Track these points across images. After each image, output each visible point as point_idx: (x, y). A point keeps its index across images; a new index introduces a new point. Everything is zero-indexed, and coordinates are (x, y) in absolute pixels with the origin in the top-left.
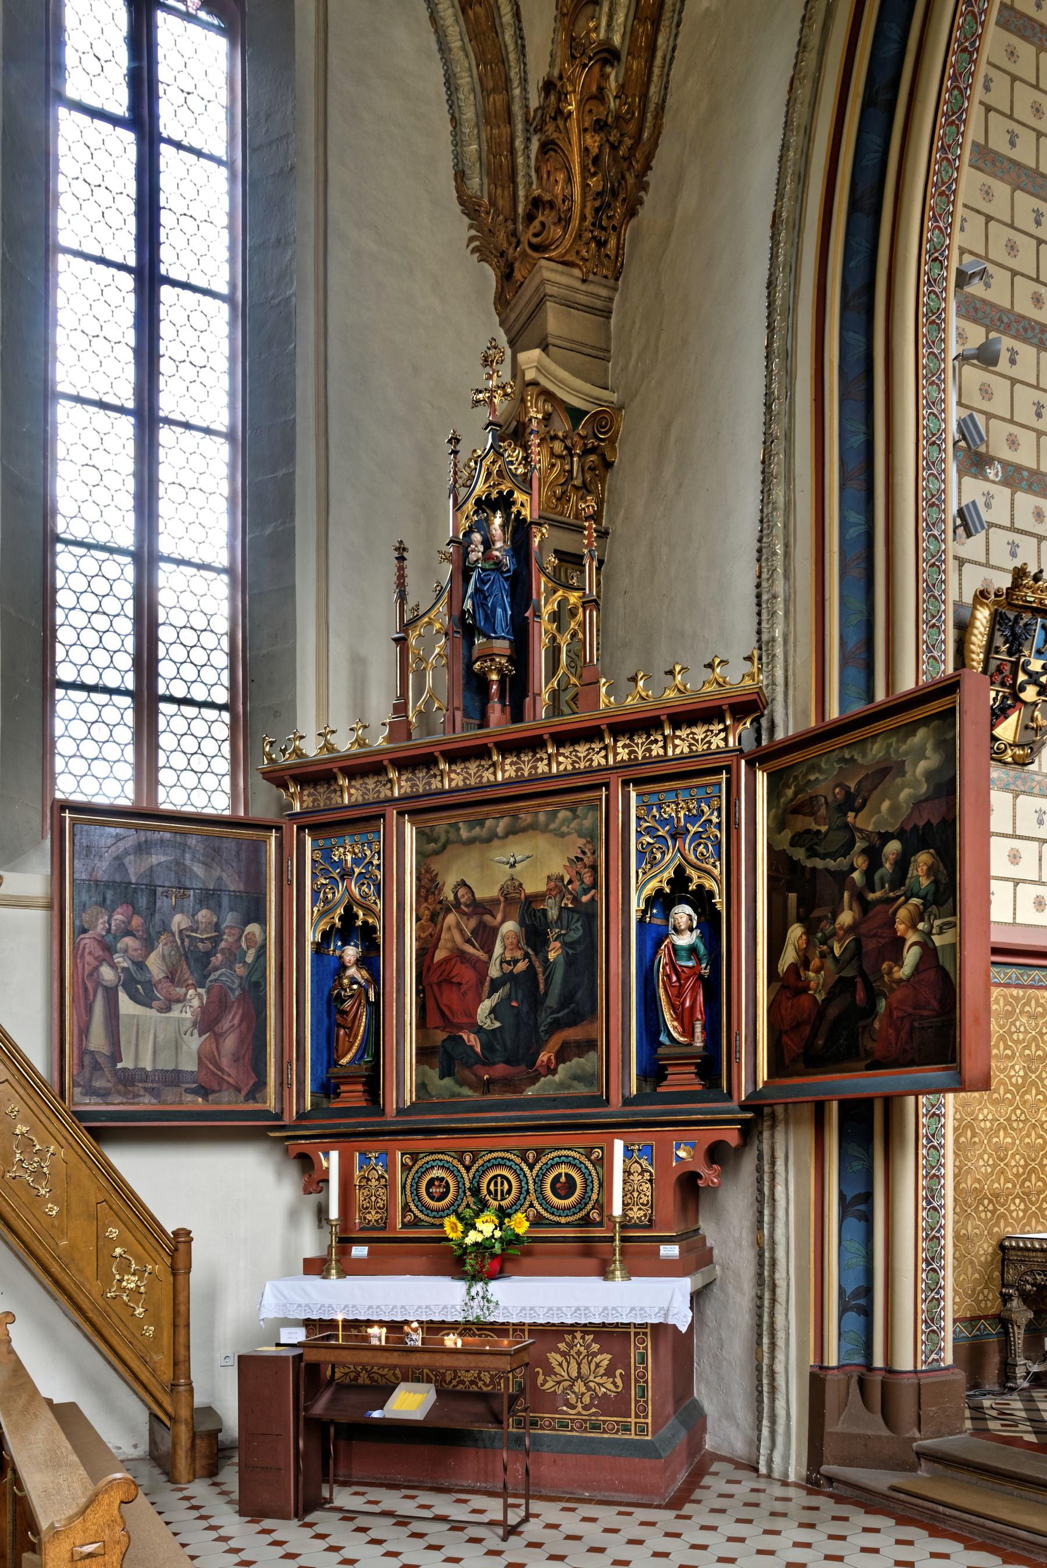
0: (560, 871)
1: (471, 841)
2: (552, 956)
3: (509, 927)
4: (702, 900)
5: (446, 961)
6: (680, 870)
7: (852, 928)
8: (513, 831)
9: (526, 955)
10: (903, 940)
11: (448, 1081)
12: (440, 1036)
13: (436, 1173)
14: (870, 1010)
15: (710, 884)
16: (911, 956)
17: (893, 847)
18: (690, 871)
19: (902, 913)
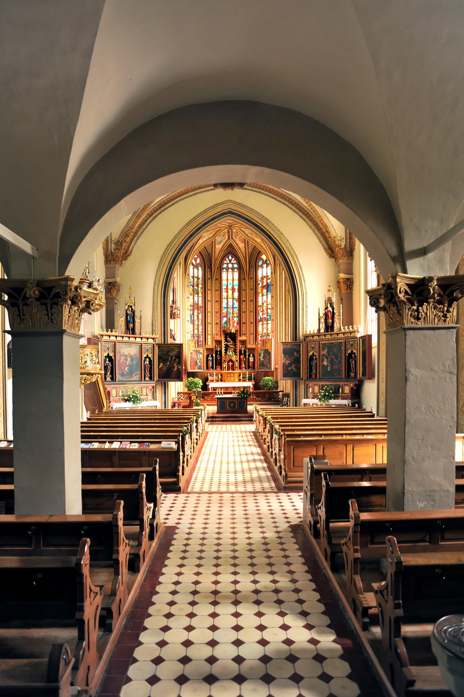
1: (125, 347)
3: (129, 359)
4: (150, 358)
8: (129, 347)
11: (122, 378)
12: (121, 372)
13: (122, 389)
14: (171, 373)
15: (151, 357)
16: (176, 368)
18: (149, 355)
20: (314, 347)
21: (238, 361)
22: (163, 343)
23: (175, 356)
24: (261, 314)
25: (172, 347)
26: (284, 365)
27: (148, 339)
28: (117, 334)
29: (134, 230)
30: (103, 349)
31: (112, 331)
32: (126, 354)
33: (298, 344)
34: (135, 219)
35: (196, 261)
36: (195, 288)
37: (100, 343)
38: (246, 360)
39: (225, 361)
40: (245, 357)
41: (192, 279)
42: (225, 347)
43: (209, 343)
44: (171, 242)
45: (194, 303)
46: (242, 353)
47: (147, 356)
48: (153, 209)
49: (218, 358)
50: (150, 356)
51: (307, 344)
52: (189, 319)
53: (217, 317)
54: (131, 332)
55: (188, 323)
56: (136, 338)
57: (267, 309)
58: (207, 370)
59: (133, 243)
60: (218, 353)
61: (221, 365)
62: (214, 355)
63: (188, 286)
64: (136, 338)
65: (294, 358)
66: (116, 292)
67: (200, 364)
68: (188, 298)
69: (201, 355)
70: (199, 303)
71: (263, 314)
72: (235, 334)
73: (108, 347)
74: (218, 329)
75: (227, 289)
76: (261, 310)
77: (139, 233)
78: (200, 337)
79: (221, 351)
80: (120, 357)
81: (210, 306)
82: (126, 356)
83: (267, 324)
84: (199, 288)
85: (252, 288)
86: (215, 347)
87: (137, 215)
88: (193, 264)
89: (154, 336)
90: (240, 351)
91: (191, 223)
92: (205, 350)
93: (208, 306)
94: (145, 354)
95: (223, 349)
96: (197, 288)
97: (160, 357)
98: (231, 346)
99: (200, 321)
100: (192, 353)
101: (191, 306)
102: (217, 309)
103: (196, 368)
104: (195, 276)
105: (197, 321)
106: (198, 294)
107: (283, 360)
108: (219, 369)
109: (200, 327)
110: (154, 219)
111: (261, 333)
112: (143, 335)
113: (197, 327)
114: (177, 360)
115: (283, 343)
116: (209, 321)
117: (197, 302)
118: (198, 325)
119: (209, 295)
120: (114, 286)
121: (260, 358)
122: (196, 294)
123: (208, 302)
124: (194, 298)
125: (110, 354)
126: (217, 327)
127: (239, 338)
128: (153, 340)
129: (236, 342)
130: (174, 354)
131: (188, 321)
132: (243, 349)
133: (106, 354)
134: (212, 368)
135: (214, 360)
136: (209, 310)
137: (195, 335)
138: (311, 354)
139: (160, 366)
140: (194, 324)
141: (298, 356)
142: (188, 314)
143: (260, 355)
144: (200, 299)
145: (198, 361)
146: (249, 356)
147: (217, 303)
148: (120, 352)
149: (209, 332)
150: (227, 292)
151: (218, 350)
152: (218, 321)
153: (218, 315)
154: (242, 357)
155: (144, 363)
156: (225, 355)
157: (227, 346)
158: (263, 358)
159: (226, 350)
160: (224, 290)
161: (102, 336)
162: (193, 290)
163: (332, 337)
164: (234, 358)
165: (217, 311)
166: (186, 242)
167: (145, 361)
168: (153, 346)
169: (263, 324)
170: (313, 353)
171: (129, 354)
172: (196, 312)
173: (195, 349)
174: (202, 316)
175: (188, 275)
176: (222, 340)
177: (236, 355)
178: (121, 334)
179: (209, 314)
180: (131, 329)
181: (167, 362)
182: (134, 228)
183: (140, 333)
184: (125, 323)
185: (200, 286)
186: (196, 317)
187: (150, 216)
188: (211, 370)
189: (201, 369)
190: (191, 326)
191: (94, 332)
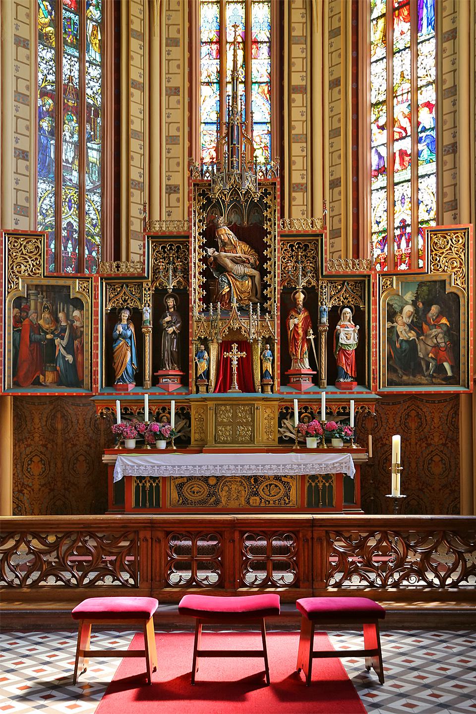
21: (277, 338)
24: (379, 138)
42: (203, 273)
45: (58, 81)
53: (173, 162)
55: (22, 163)
57: (414, 108)
58: (110, 390)
60: (171, 302)
61: (183, 360)
67: (69, 358)
69: (76, 313)
70: (89, 91)
71: (392, 140)
75: (220, 41)
76: (382, 122)
81: (142, 112)
83: (416, 178)
84: (90, 25)
85: (336, 25)
86: (156, 271)
90: (288, 293)
92: (101, 287)
93: (132, 105)
95: (196, 282)
98: (240, 269)
102: (173, 127)
103: (50, 377)
106: (81, 45)
108: (174, 386)
111: (383, 225)
116: (135, 175)
119: (136, 61)
121: (391, 330)
122: (72, 45)
123: (132, 90)
124: (58, 60)
126: (173, 203)
129: (266, 246)
131: (22, 155)
132: (302, 283)
136: (136, 126)
137: (64, 233)
140: (58, 181)
142: (22, 124)
143: (392, 315)
144: (95, 72)
145: (60, 344)
146: (335, 315)
147: (174, 99)
150: (221, 54)
154: (297, 321)
156: (206, 311)
159: (211, 295)
160: (205, 49)
165: (173, 132)
169: (391, 186)
172: (70, 127)
173: (45, 282)
174: (102, 151)
176: (188, 237)
177: (264, 311)
179: (135, 144)
185: (94, 13)
186: (68, 154)
188: (131, 387)
189: (79, 384)
190: (44, 187)
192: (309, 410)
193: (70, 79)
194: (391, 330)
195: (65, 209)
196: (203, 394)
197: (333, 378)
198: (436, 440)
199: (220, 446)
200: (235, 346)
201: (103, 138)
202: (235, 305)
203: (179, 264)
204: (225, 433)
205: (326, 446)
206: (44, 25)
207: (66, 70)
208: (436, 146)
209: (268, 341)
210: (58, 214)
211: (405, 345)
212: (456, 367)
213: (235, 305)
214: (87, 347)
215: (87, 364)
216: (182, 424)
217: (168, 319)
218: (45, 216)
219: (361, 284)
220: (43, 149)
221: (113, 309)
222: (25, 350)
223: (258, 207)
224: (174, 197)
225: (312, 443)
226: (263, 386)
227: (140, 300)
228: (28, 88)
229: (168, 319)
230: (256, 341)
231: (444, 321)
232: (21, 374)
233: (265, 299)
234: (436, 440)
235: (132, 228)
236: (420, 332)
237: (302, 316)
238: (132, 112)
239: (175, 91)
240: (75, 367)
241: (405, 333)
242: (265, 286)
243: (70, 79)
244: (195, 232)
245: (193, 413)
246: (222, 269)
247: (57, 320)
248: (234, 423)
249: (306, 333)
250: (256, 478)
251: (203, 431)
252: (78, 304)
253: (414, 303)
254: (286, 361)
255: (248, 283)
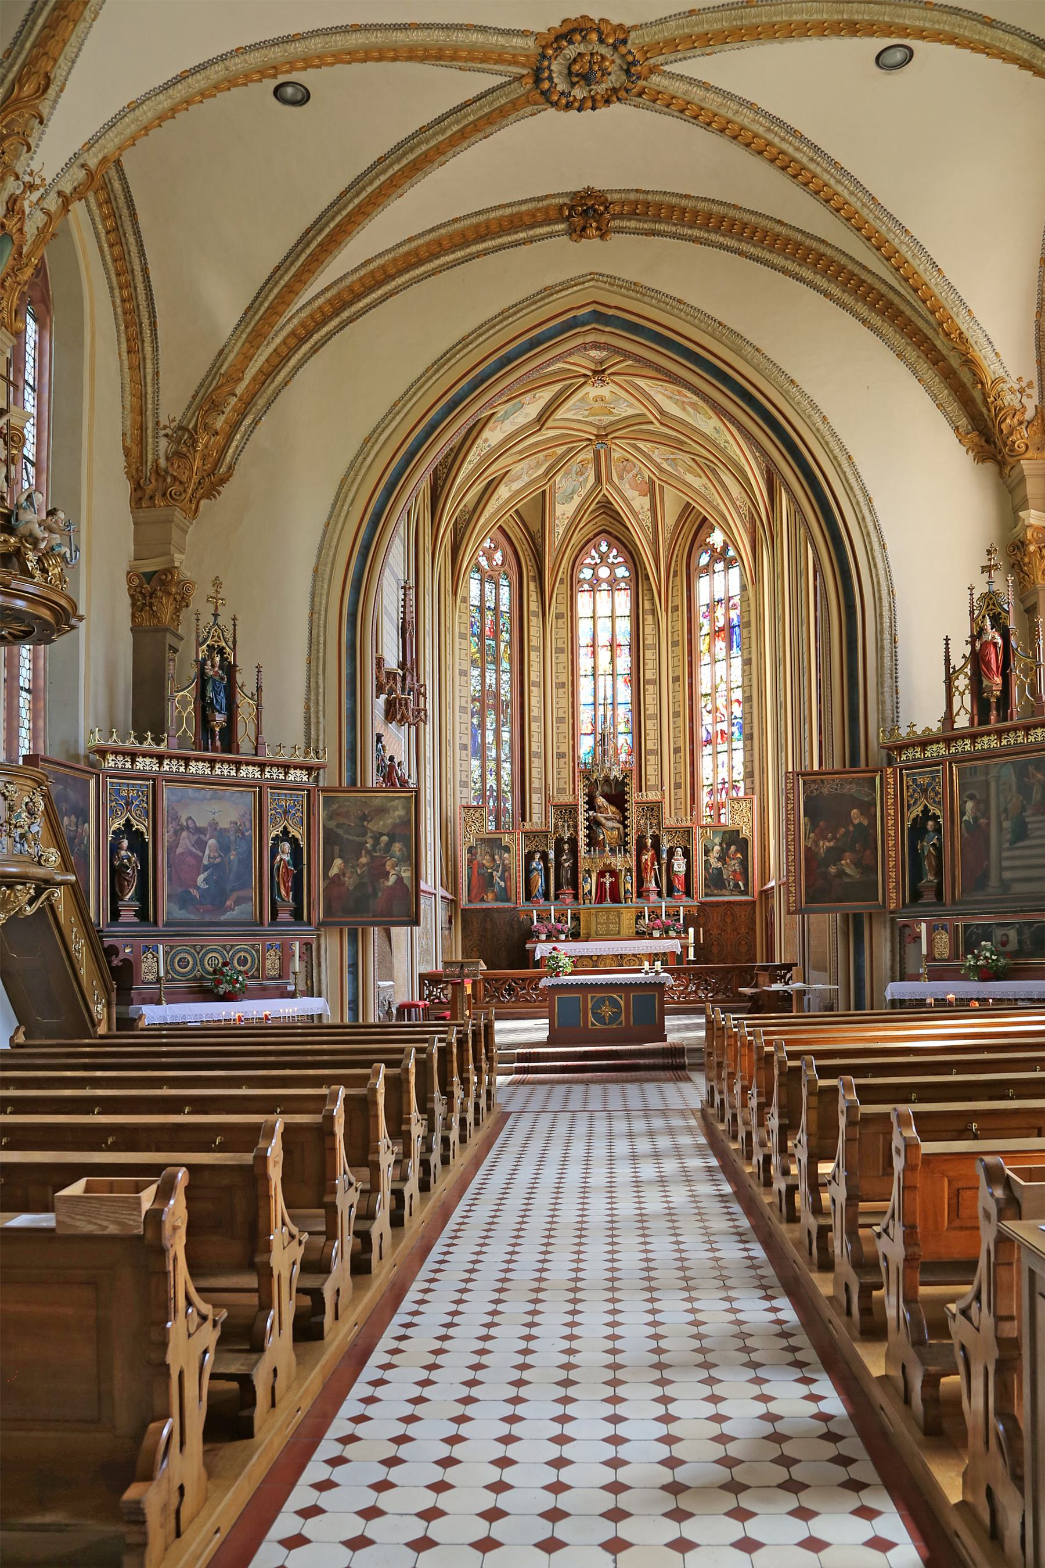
0: (235, 819)
1: (194, 799)
2: (232, 857)
4: (294, 841)
5: (182, 854)
6: (285, 828)
7: (364, 865)
8: (213, 798)
9: (220, 856)
10: (389, 873)
15: (299, 836)
17: (385, 838)
18: (290, 829)
19: (389, 863)
20: (929, 785)
21: (634, 869)
22: (345, 784)
23: (388, 835)
25: (377, 802)
26: (811, 855)
27: (286, 767)
28: (163, 747)
29: (240, 389)
30: (105, 805)
31: (141, 739)
32: (198, 824)
33: (864, 778)
34: (243, 345)
35: (490, 559)
36: (488, 642)
37: (92, 783)
38: (660, 869)
39: (588, 872)
40: (658, 856)
41: (477, 616)
42: (587, 828)
43: (535, 818)
44: (377, 428)
46: (646, 847)
47: (285, 831)
48: (311, 316)
49: (566, 865)
50: (293, 832)
51: (901, 775)
52: (467, 740)
54: (218, 743)
56: (238, 764)
59: (238, 436)
60: (566, 846)
61: (575, 884)
62: (552, 855)
63: (463, 636)
64: (238, 764)
65: (851, 828)
66: (171, 608)
67: (502, 884)
68: (463, 673)
69: (506, 855)
70: (502, 692)
72: (623, 784)
73: (126, 798)
74: (566, 773)
77: (261, 402)
78: (506, 799)
79: (573, 841)
80: (177, 833)
82: (199, 831)
84: (502, 645)
86: (556, 826)
87: (248, 330)
88: (479, 569)
89: (311, 760)
91: (449, 359)
92: (521, 837)
93: (532, 698)
94: (275, 824)
96: (493, 643)
97: (331, 838)
98: (610, 824)
99: (506, 749)
100: (476, 848)
101: (474, 700)
102: (561, 711)
104: (488, 604)
105: (494, 746)
106: (497, 661)
107: (807, 838)
108: (569, 899)
109: (507, 766)
110: (315, 350)
112: (269, 755)
113: (494, 768)
114: (397, 847)
115: (803, 775)
116: (534, 748)
117: (494, 686)
118: (498, 761)
120: (163, 583)
124: (483, 675)
125: (134, 822)
127: (633, 797)
128: (309, 775)
129: (627, 810)
130: (384, 825)
131: (464, 747)
133: (118, 824)
134: (546, 896)
135: (552, 870)
136: (536, 712)
137: (488, 793)
138: (918, 810)
139: (334, 871)
141: (866, 823)
144: (505, 677)
146: (671, 853)
147: (561, 690)
148: (176, 818)
149: (536, 784)
151: (566, 838)
152: (564, 748)
153: (565, 728)
154: (647, 857)
155: (273, 857)
156: (589, 851)
157: (594, 825)
158: (719, 859)
159: (593, 841)
161: (102, 752)
162: (481, 651)
163: (1004, 742)
164: (618, 862)
166: (432, 427)
167: (274, 853)
168: (308, 796)
170: (926, 810)
171: (214, 825)
174: (511, 732)
175: (465, 600)
177: (626, 851)
178: (179, 748)
179: (535, 726)
180: (217, 729)
181: (359, 856)
182: (241, 379)
183: (256, 748)
184: (195, 710)
185: (505, 636)
186: (490, 737)
187: (303, 341)
189: (508, 900)
190: (475, 763)
191: (77, 741)
192: (655, 914)
193: (490, 686)
194: (707, 861)
195: (488, 776)
196: (587, 905)
197: (670, 893)
198: (743, 930)
199: (599, 937)
200: (608, 874)
201: (512, 722)
202: (607, 849)
203: (571, 823)
204: (602, 929)
205: (665, 934)
206: (474, 653)
207: (488, 680)
208: (741, 728)
209: (629, 870)
210: (483, 777)
211: (715, 871)
212: (746, 885)
213: (607, 849)
214: (513, 877)
215: (513, 887)
216: (574, 923)
217: (565, 857)
218: (475, 783)
219: (688, 832)
220: (474, 737)
221: (529, 852)
222: (475, 880)
223: (621, 784)
224: (562, 761)
225: (656, 934)
226: (625, 899)
227: (547, 845)
228: (467, 702)
229: (565, 857)
230: (621, 870)
231: (739, 855)
232: (473, 895)
233: (627, 843)
234: (743, 930)
235: (533, 786)
236: (724, 863)
237: (650, 853)
238: (532, 704)
239: (562, 685)
240: (505, 890)
241: (715, 864)
242: (626, 835)
243: (490, 686)
244: (581, 802)
245: (582, 917)
246: (599, 824)
247: (494, 860)
248: (608, 922)
249: (653, 865)
250: (621, 956)
251: (588, 928)
252: (507, 849)
253: (721, 845)
254: (640, 882)
255: (616, 832)
